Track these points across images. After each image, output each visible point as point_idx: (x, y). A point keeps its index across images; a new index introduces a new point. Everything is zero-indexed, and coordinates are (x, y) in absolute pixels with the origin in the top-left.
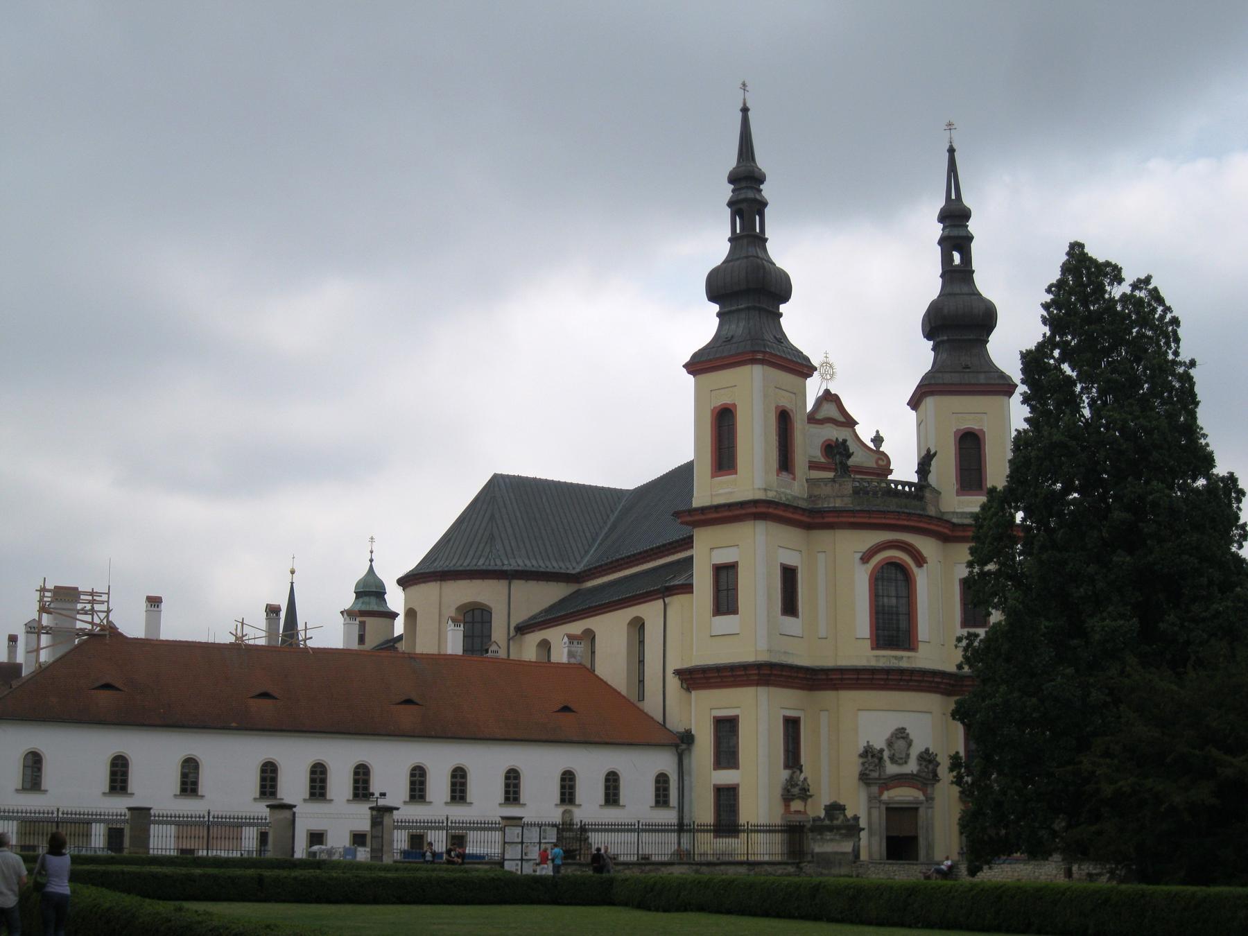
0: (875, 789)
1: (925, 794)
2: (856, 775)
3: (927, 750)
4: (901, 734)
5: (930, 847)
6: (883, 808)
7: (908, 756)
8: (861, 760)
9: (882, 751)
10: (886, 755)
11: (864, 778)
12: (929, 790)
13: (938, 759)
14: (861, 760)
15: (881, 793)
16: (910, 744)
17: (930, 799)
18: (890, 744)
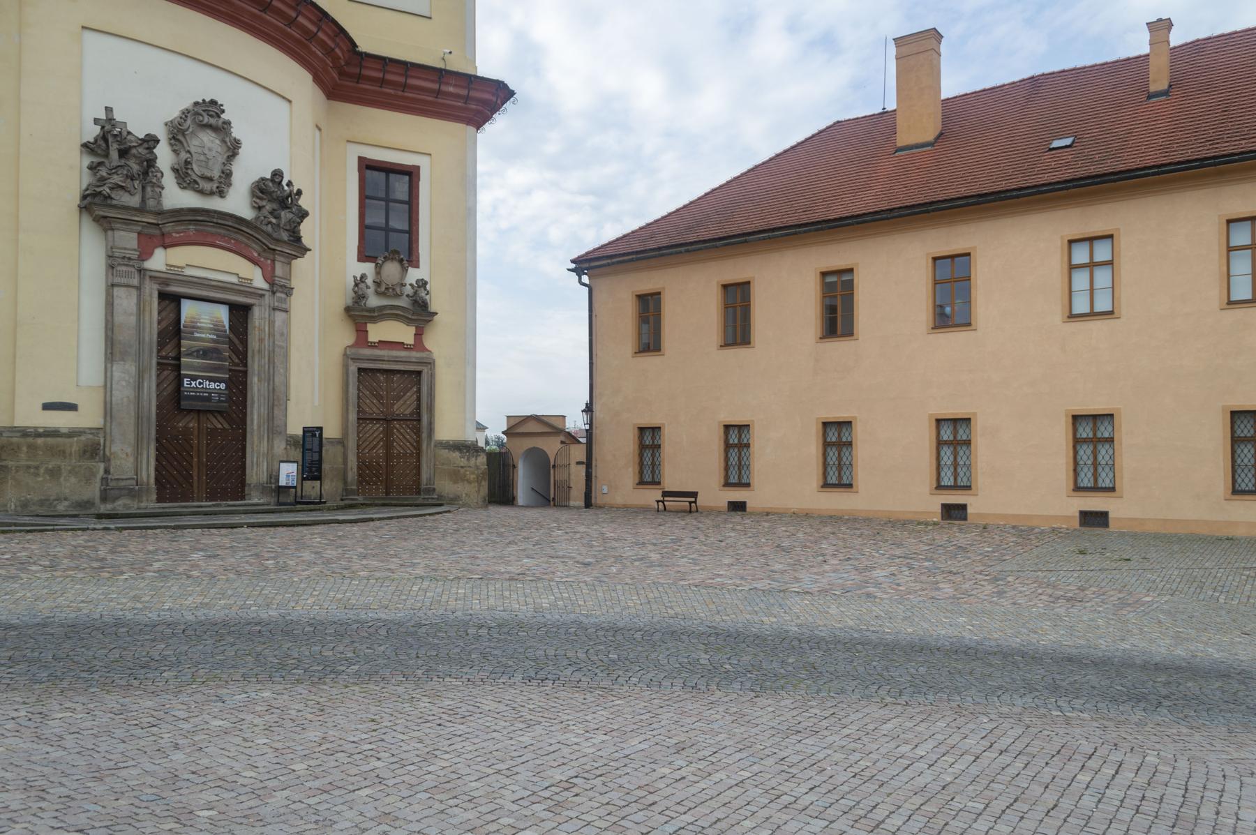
0: (128, 240)
1: (270, 278)
2: (73, 196)
3: (277, 174)
4: (207, 116)
5: (277, 400)
6: (151, 290)
7: (227, 175)
8: (87, 160)
9: (151, 141)
10: (164, 156)
11: (95, 204)
12: (279, 270)
13: (303, 202)
14: (87, 160)
15: (146, 254)
16: (233, 149)
17: (280, 288)
18: (177, 134)
